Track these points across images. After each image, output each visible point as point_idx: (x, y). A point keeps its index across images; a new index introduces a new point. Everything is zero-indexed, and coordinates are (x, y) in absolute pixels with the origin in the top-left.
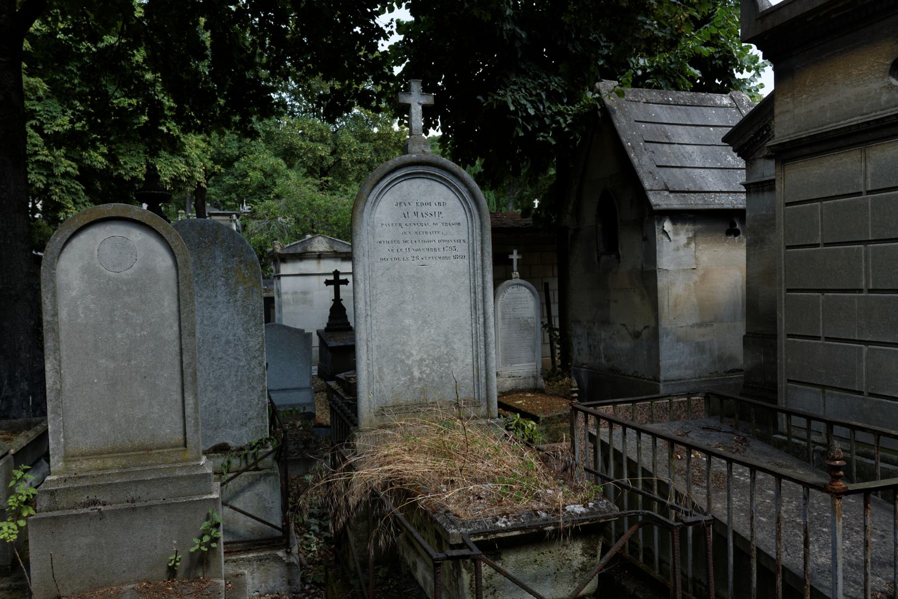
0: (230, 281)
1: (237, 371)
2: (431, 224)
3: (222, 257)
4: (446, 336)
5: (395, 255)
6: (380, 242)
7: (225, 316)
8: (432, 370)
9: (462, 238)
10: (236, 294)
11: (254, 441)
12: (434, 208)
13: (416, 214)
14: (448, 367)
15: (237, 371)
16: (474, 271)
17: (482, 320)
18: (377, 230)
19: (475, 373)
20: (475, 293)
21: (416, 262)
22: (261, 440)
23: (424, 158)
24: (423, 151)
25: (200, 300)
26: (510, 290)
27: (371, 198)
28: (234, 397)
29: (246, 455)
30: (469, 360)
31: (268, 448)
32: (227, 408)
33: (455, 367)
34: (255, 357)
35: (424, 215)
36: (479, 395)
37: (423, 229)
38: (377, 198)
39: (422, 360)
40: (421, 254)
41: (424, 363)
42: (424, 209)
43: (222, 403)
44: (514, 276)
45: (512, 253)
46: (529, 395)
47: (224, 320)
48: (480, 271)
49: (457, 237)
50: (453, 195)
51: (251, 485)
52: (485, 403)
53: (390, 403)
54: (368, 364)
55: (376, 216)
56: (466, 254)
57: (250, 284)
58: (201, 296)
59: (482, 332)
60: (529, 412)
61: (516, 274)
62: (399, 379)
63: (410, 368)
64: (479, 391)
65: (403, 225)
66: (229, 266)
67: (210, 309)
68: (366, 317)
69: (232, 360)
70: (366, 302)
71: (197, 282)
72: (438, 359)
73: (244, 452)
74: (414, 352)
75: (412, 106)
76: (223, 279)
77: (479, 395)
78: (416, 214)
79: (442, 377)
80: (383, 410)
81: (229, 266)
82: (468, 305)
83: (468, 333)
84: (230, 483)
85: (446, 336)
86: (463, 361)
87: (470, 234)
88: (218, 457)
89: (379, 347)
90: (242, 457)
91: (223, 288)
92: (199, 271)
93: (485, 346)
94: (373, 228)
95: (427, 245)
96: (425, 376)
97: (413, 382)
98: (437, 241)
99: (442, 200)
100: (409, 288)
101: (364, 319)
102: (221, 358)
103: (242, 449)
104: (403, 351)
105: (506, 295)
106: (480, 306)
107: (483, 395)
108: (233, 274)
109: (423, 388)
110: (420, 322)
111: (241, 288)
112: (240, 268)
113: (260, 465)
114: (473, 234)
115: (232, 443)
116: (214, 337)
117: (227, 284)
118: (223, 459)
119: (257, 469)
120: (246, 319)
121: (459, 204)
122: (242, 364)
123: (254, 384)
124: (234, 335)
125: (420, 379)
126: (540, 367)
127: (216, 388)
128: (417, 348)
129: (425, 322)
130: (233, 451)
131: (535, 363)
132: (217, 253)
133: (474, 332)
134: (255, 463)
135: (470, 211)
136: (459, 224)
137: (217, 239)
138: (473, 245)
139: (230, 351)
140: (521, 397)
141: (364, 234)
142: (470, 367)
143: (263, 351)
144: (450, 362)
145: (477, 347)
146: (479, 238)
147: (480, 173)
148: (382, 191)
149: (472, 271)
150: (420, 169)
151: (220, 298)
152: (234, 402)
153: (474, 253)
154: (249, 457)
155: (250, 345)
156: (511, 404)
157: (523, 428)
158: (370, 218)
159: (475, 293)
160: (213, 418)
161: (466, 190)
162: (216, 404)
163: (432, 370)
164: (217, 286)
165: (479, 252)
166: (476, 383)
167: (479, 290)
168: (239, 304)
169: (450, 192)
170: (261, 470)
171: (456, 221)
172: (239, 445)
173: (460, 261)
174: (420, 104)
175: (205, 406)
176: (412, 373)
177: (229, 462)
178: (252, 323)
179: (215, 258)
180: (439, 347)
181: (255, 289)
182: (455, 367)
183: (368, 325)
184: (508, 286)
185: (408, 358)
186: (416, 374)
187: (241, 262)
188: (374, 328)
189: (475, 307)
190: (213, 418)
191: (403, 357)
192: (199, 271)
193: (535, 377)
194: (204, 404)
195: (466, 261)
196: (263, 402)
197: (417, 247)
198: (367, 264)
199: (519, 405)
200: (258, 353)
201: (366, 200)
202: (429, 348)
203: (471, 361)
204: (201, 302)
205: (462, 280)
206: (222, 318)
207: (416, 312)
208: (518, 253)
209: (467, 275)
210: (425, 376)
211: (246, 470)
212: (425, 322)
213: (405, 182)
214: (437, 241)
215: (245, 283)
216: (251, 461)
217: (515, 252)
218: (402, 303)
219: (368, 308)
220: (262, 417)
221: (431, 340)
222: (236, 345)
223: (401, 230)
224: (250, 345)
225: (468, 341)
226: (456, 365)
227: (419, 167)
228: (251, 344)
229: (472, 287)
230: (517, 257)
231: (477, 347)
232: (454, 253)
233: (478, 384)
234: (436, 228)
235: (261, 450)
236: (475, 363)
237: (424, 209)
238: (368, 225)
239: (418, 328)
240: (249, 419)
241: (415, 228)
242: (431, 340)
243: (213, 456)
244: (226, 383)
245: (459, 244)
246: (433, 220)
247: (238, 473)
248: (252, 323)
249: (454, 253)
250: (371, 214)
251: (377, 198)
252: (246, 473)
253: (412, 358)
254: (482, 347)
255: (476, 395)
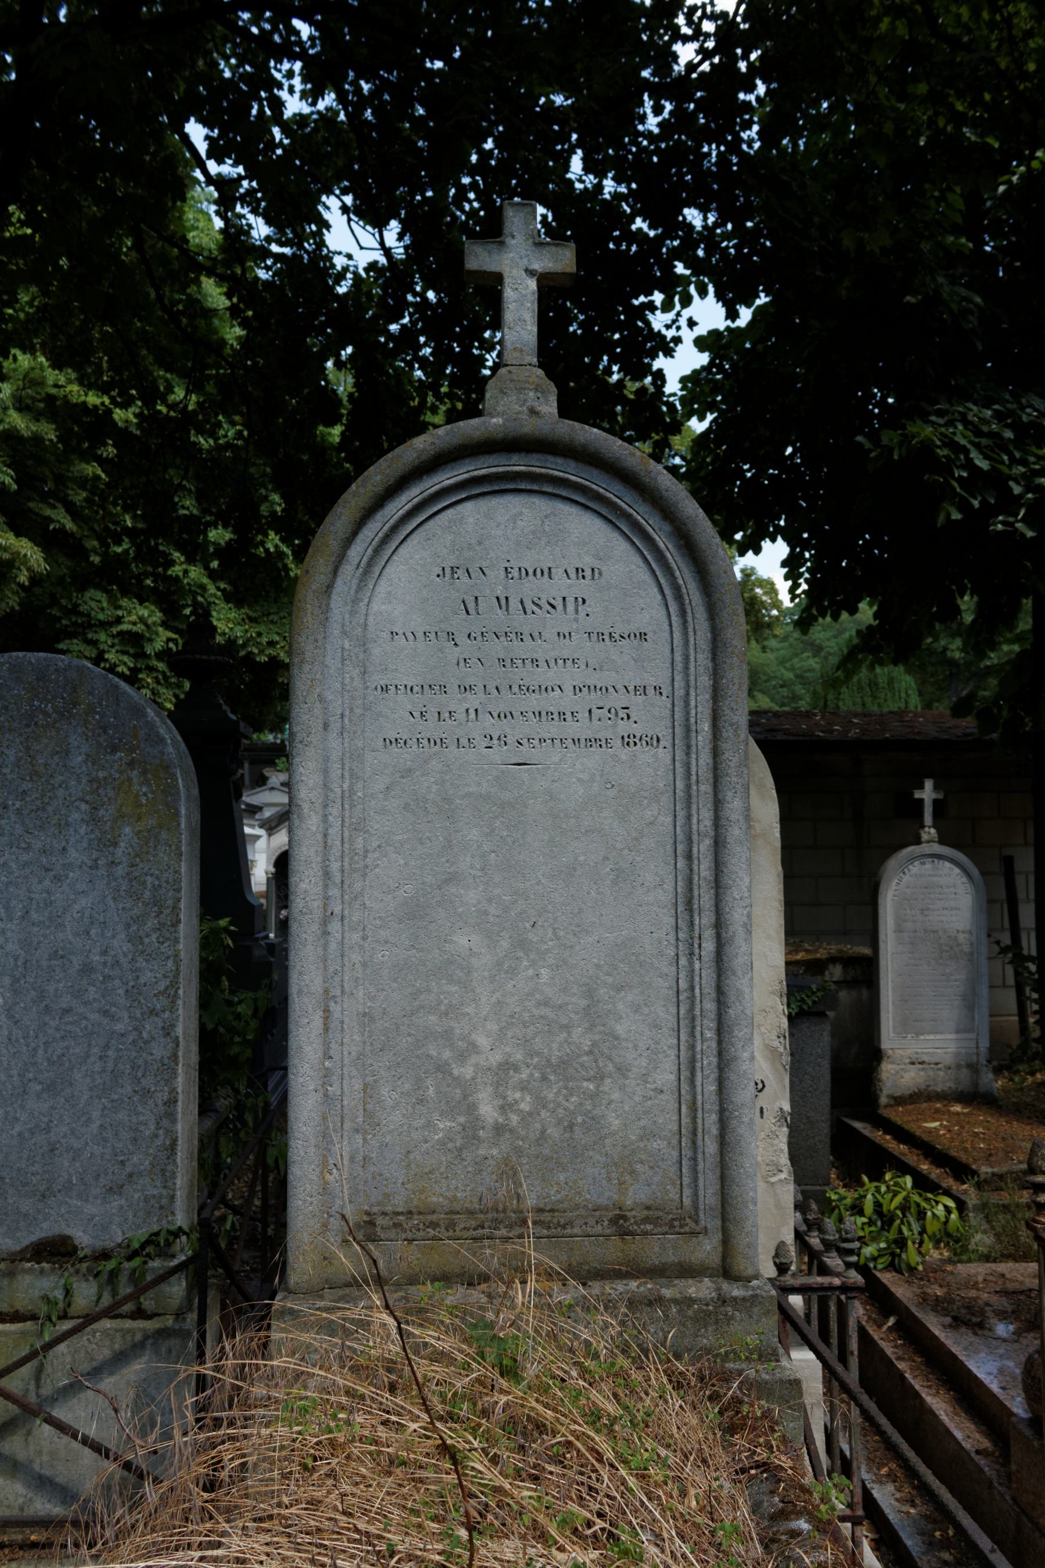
0: (102, 812)
1: (107, 1047)
2: (550, 634)
3: (85, 749)
4: (590, 993)
5: (431, 728)
6: (385, 689)
7: (84, 902)
8: (541, 1102)
9: (651, 681)
10: (115, 844)
11: (142, 1234)
12: (560, 586)
13: (501, 603)
14: (594, 1096)
15: (107, 1047)
16: (688, 787)
17: (709, 946)
18: (376, 651)
19: (686, 1121)
20: (689, 857)
21: (497, 754)
22: (157, 1234)
23: (529, 427)
24: (533, 412)
25: (25, 857)
26: (915, 868)
27: (357, 551)
28: (96, 1114)
29: (113, 1275)
30: (666, 1076)
31: (173, 1256)
32: (76, 1144)
33: (616, 1095)
34: (153, 1012)
35: (530, 607)
36: (696, 1194)
37: (524, 649)
38: (377, 551)
39: (507, 1066)
40: (515, 730)
41: (515, 1078)
42: (530, 588)
43: (64, 1129)
44: (925, 837)
45: (921, 787)
46: (957, 1108)
47: (81, 912)
48: (706, 788)
49: (632, 678)
50: (621, 546)
51: (120, 1359)
52: (713, 1224)
53: (399, 1203)
54: (327, 1074)
55: (375, 607)
56: (664, 732)
57: (152, 822)
58: (28, 848)
59: (709, 989)
60: (953, 1153)
61: (929, 832)
62: (429, 1125)
63: (467, 1089)
64: (695, 1180)
65: (462, 639)
66: (101, 774)
67: (47, 882)
68: (325, 922)
69: (94, 1016)
70: (327, 874)
71: (19, 812)
72: (563, 1066)
73: (111, 1265)
74: (482, 1041)
75: (506, 275)
76: (84, 807)
77: (696, 1194)
78: (501, 603)
79: (571, 1127)
80: (371, 1223)
81: (101, 774)
82: (664, 895)
83: (664, 986)
84: (62, 1347)
85: (590, 993)
86: (644, 1078)
87: (679, 666)
88: (42, 1272)
89: (367, 1018)
90: (105, 1276)
91: (83, 830)
92: (26, 786)
93: (719, 1031)
94: (363, 644)
95: (534, 702)
96: (515, 1119)
97: (475, 1137)
98: (568, 688)
99: (587, 562)
100: (474, 834)
101: (315, 927)
102: (67, 1011)
103: (105, 1255)
104: (447, 1035)
105: (906, 878)
106: (705, 898)
107: (709, 1195)
108: (111, 794)
109: (506, 1161)
110: (505, 944)
111: (127, 830)
112: (130, 780)
113: (148, 1303)
114: (686, 668)
115: (84, 1238)
116: (54, 955)
117: (93, 819)
118: (53, 1278)
119: (140, 1314)
120: (136, 912)
121: (645, 576)
122: (119, 1027)
123: (148, 1082)
124: (104, 953)
125: (499, 1129)
126: (985, 1044)
127: (51, 1088)
128: (492, 1026)
129: (521, 944)
130: (81, 1260)
131: (973, 1036)
132: (74, 740)
133: (683, 984)
134: (134, 1297)
135: (679, 597)
136: (643, 636)
137: (75, 704)
138: (687, 703)
139: (92, 993)
140: (937, 1111)
141: (332, 662)
142: (668, 1100)
143: (176, 996)
144: (599, 1077)
145: (692, 1034)
146: (705, 681)
147: (870, 627)
148: (394, 529)
149: (680, 785)
150: (518, 464)
151: (73, 855)
152: (94, 1127)
153: (688, 729)
154: (123, 1278)
155: (142, 981)
156: (912, 1127)
157: (921, 1215)
158: (353, 613)
159: (689, 857)
160: (37, 1168)
161: (667, 527)
162: (48, 1130)
163: (541, 1102)
164: (68, 824)
165: (706, 726)
166: (687, 1152)
167: (703, 847)
168: (120, 871)
169: (615, 536)
170: (150, 1317)
171: (634, 627)
172: (99, 1244)
173: (644, 754)
174: (530, 273)
175: (20, 1134)
176: (472, 1108)
177: (68, 1292)
178: (151, 923)
179: (67, 753)
180: (567, 1028)
181: (164, 835)
182: (616, 1095)
183: (333, 946)
184: (912, 859)
185: (462, 1057)
186: (488, 1111)
187: (131, 764)
188: (356, 957)
189: (689, 903)
190: (37, 1168)
191: (447, 1054)
192: (26, 786)
193: (973, 1068)
194: (18, 1128)
195: (664, 755)
196: (168, 1131)
197: (503, 707)
198: (335, 756)
199: (930, 1131)
200: (163, 1001)
201: (341, 558)
202: (530, 1031)
203: (673, 1077)
204: (26, 864)
205: (648, 814)
206: (77, 907)
207: (493, 910)
208: (936, 788)
209: (666, 800)
210: (515, 1119)
211: (110, 1313)
212: (521, 944)
213: (469, 505)
214: (568, 688)
215: (139, 819)
216: (125, 1289)
217: (929, 784)
218: (447, 881)
219: (334, 892)
220: (163, 1171)
221: (539, 1004)
222: (107, 978)
223: (454, 654)
224: (142, 981)
225: (666, 1014)
226: (623, 1088)
227: (515, 458)
228: (147, 977)
229: (681, 836)
230: (934, 796)
231: (692, 1034)
232: (624, 728)
233: (694, 1159)
234: (566, 649)
235: (155, 1264)
236: (685, 1087)
237: (530, 588)
238: (344, 633)
239: (499, 964)
240: (130, 1176)
241: (497, 648)
242: (539, 1004)
243: (30, 1271)
244: (77, 1076)
245: (640, 699)
246: (554, 622)
247: (89, 1319)
248: (151, 923)
249: (624, 728)
250: (356, 601)
251: (377, 551)
252: (107, 1324)
253: (473, 1059)
254: (709, 1034)
255: (687, 1192)
